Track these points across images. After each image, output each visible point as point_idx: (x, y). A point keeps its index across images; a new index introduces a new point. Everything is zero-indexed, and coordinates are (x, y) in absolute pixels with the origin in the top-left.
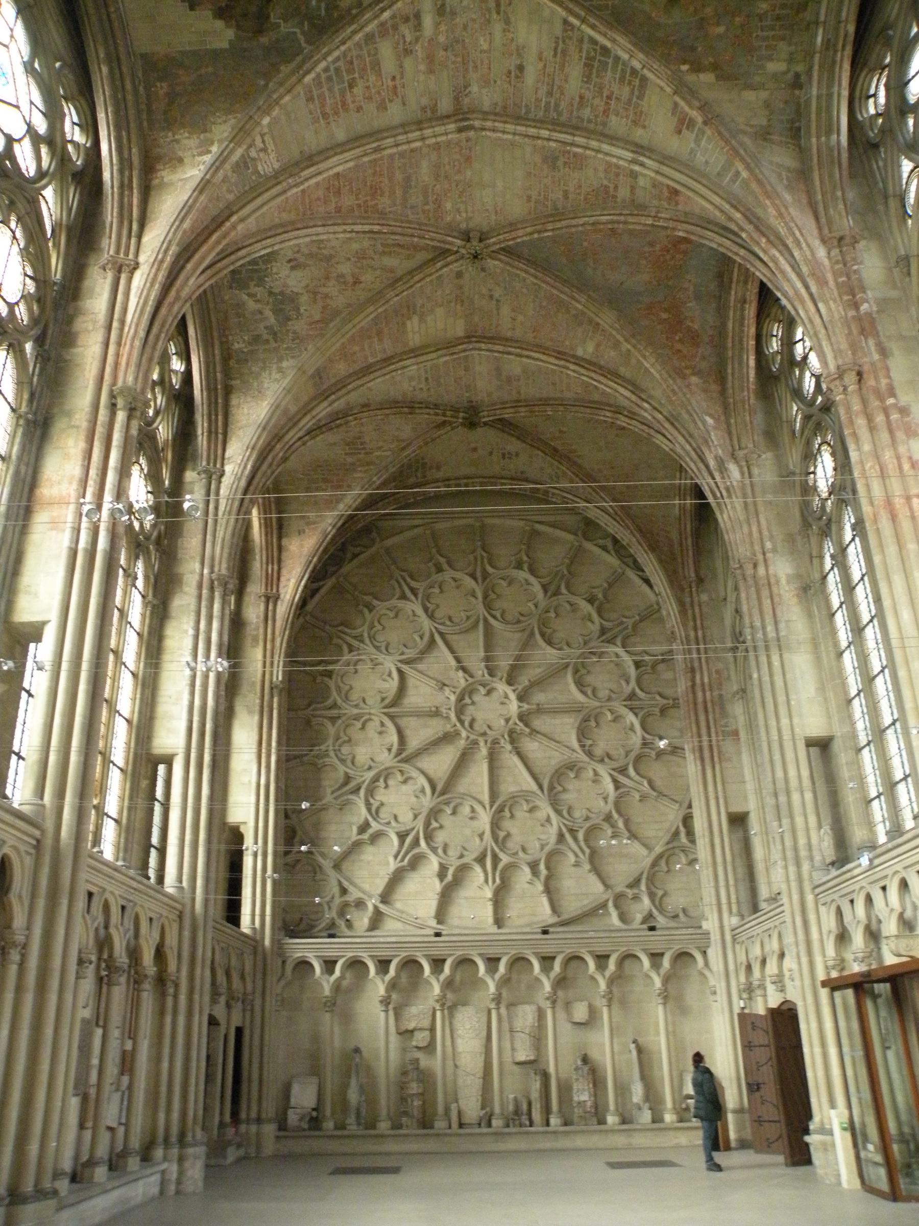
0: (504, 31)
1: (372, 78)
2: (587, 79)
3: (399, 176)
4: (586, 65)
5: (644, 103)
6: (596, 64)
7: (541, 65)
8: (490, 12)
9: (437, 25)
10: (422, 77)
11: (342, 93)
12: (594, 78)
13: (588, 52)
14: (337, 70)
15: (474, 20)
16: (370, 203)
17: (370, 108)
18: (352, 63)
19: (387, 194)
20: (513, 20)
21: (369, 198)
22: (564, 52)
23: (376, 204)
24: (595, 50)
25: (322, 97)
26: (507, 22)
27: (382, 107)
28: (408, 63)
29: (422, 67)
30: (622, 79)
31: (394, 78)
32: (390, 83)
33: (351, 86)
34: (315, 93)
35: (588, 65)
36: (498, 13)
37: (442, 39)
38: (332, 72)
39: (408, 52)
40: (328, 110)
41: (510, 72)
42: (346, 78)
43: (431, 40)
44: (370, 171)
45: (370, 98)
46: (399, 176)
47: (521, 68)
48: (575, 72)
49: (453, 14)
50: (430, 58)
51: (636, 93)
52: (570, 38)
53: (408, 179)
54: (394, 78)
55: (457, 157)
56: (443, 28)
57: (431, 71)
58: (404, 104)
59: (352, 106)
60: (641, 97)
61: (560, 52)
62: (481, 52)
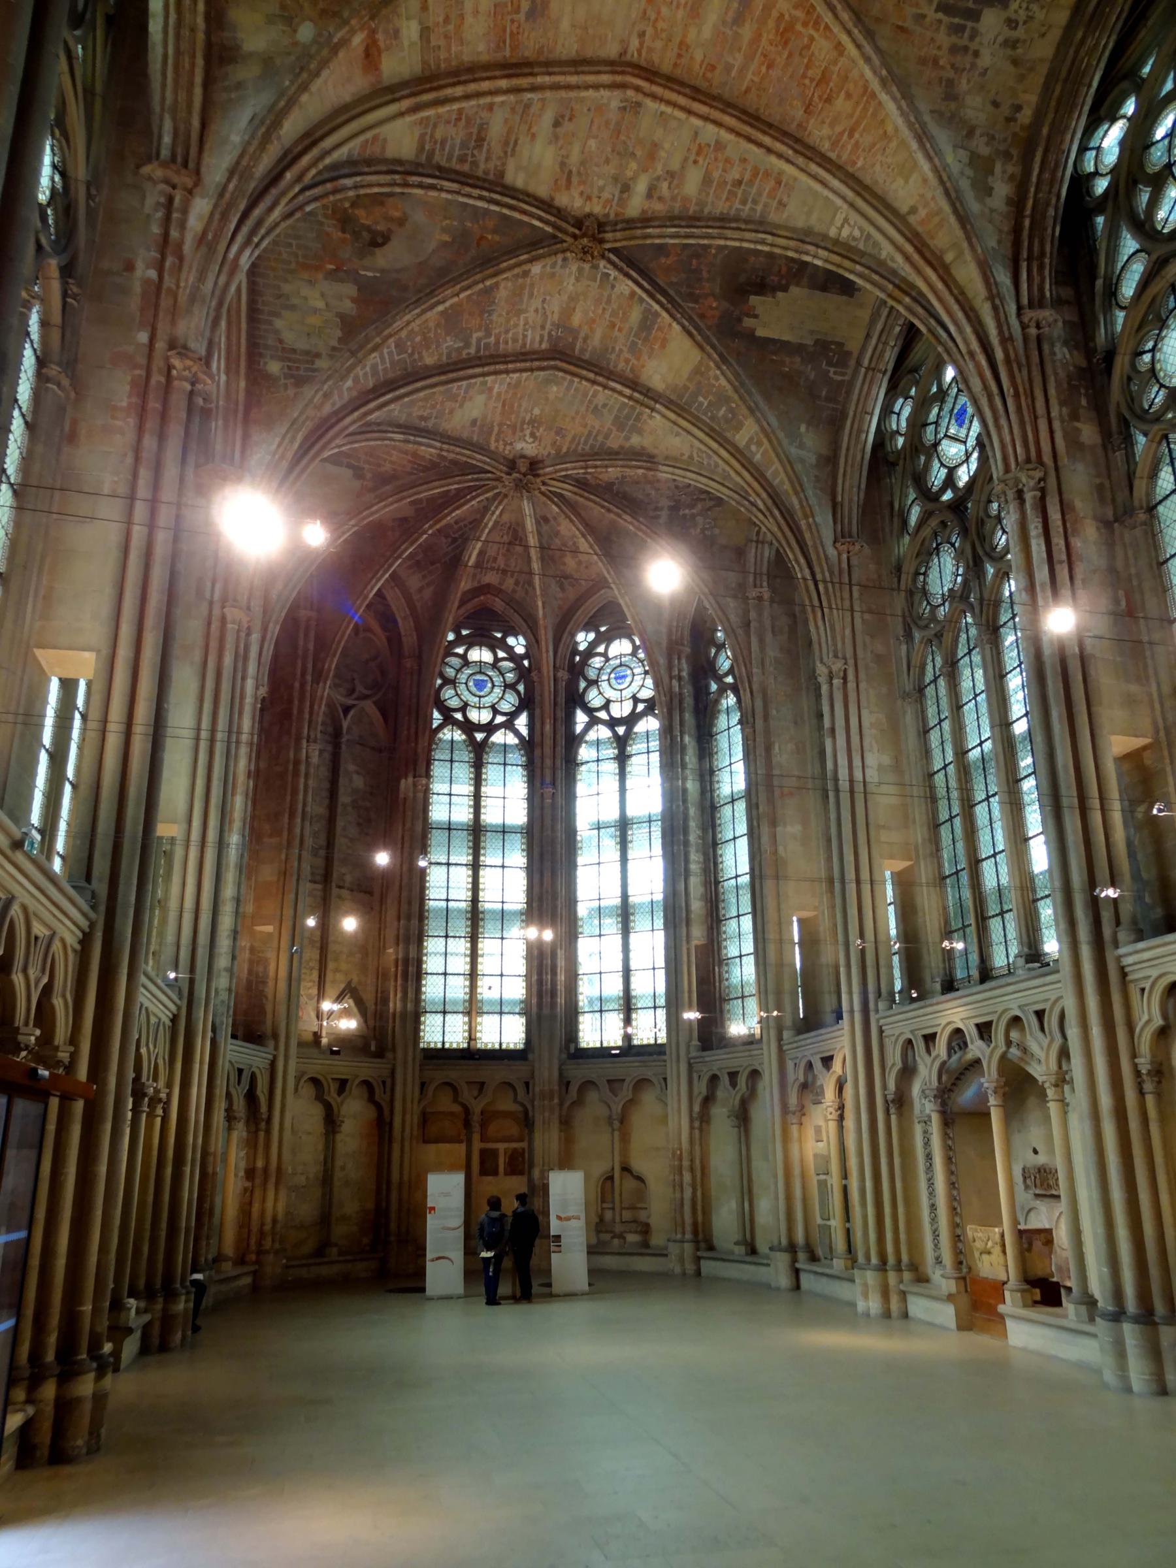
0: (567, 156)
1: (716, 175)
2: (483, 127)
3: (747, 32)
4: (484, 140)
5: (417, 134)
6: (473, 144)
7: (534, 130)
8: (579, 173)
9: (634, 179)
10: (667, 146)
11: (751, 182)
12: (475, 130)
13: (481, 152)
14: (744, 202)
15: (597, 165)
16: (799, 14)
17: (729, 152)
18: (727, 199)
19: (775, 14)
20: (557, 167)
21: (799, 27)
22: (506, 143)
23: (796, 7)
24: (473, 155)
25: (771, 196)
26: (563, 164)
27: (719, 146)
28: (675, 165)
29: (663, 154)
30: (443, 142)
31: (695, 162)
32: (701, 160)
33: (740, 182)
34: (775, 204)
35: (480, 140)
36: (570, 172)
37: (634, 165)
38: (749, 205)
39: (671, 175)
40: (772, 183)
41: (570, 119)
42: (740, 192)
43: (645, 170)
44: (774, 73)
45: (727, 160)
46: (747, 32)
47: (557, 124)
48: (496, 128)
49: (616, 179)
50: (652, 156)
51: (428, 138)
52: (499, 158)
53: (739, 20)
54: (695, 162)
55: (665, 11)
56: (629, 174)
57: (655, 145)
58: (696, 133)
59: (749, 168)
60: (422, 137)
61: (510, 145)
62: (596, 137)
